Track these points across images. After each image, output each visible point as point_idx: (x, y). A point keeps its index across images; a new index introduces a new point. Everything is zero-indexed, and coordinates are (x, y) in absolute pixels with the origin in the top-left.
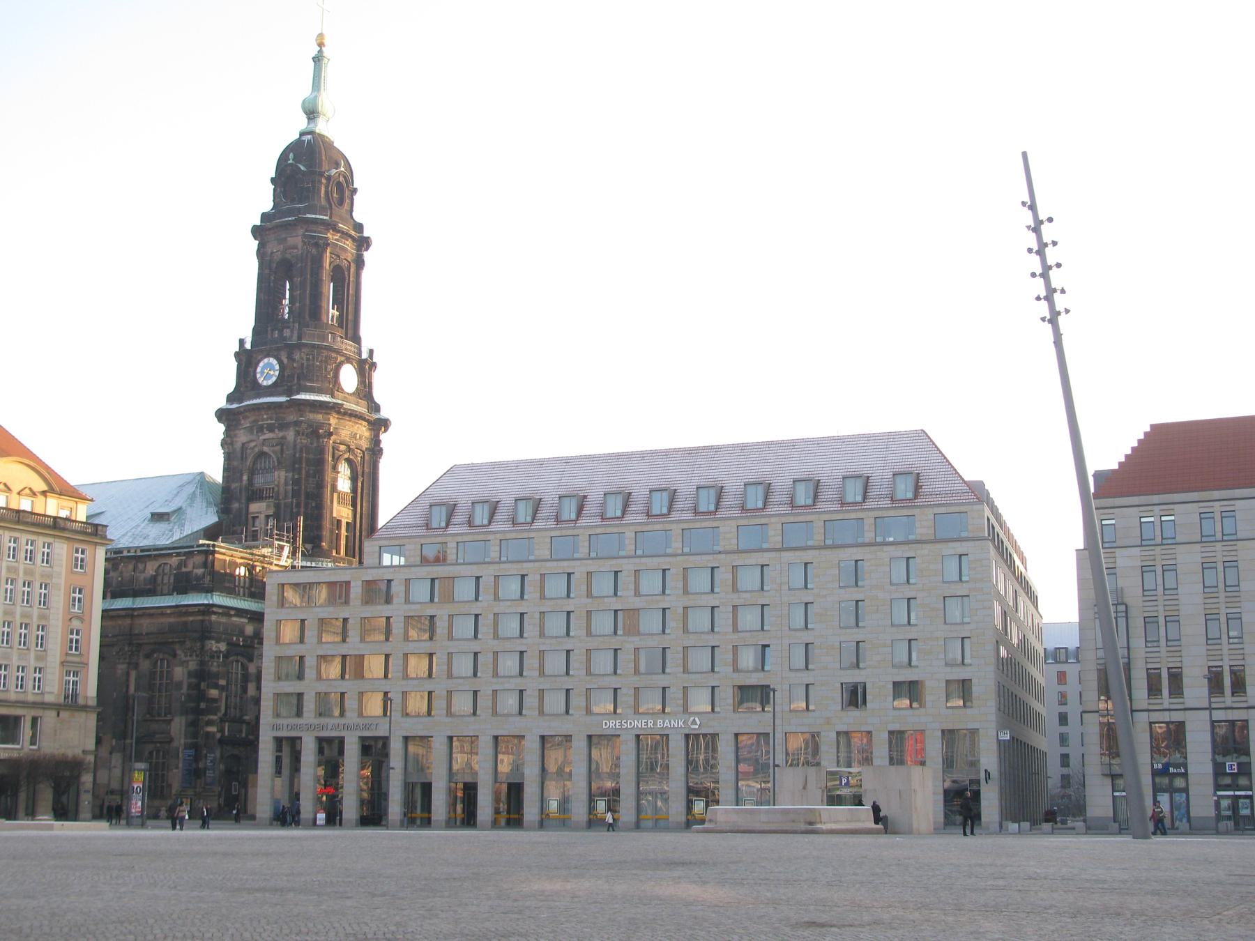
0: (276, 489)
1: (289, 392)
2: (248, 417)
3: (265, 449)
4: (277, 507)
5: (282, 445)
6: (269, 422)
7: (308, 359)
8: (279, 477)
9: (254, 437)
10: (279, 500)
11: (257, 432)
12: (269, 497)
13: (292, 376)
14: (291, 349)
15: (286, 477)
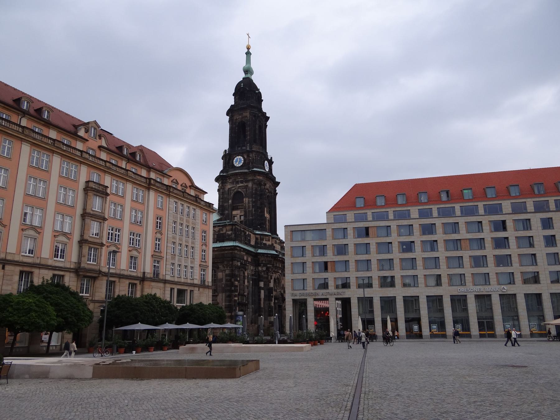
0: (245, 205)
1: (248, 169)
2: (232, 178)
3: (240, 190)
4: (245, 212)
5: (246, 189)
6: (241, 180)
7: (255, 157)
8: (246, 200)
9: (234, 185)
10: (246, 209)
11: (236, 184)
12: (241, 208)
13: (249, 163)
14: (248, 153)
15: (248, 200)
